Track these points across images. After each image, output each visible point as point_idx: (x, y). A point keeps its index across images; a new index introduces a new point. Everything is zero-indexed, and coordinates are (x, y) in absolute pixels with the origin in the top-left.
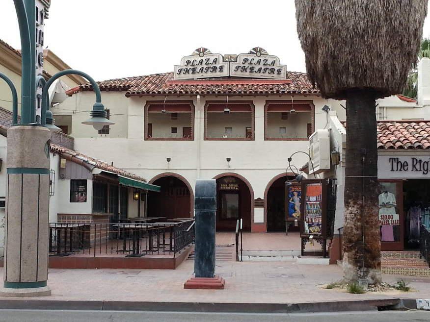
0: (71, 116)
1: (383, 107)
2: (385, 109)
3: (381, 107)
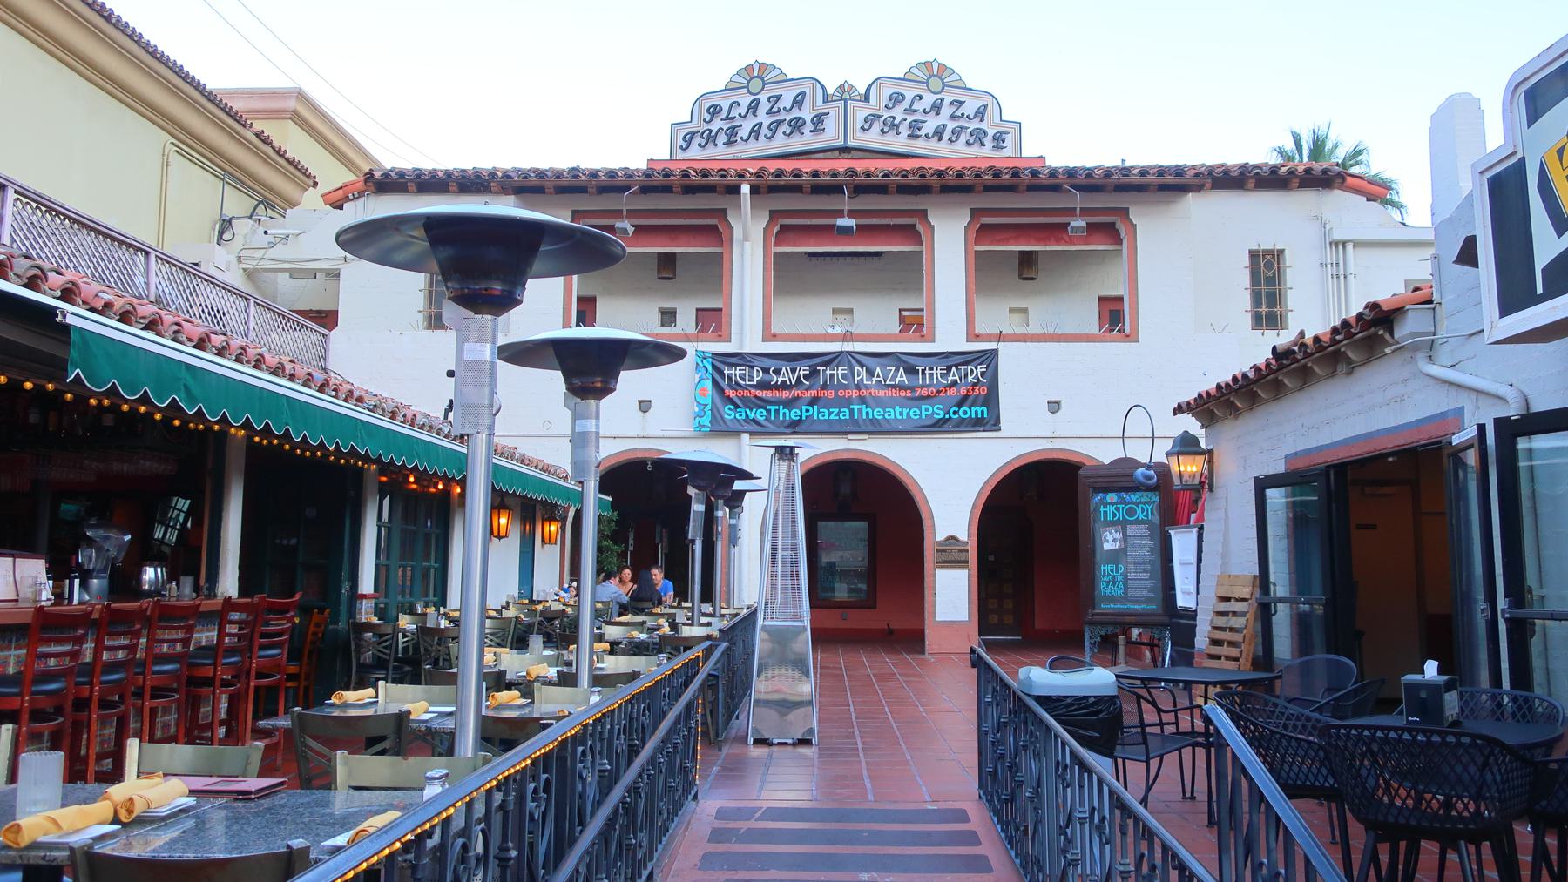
0: (335, 275)
1: (1344, 243)
2: (1350, 247)
3: (1336, 244)
